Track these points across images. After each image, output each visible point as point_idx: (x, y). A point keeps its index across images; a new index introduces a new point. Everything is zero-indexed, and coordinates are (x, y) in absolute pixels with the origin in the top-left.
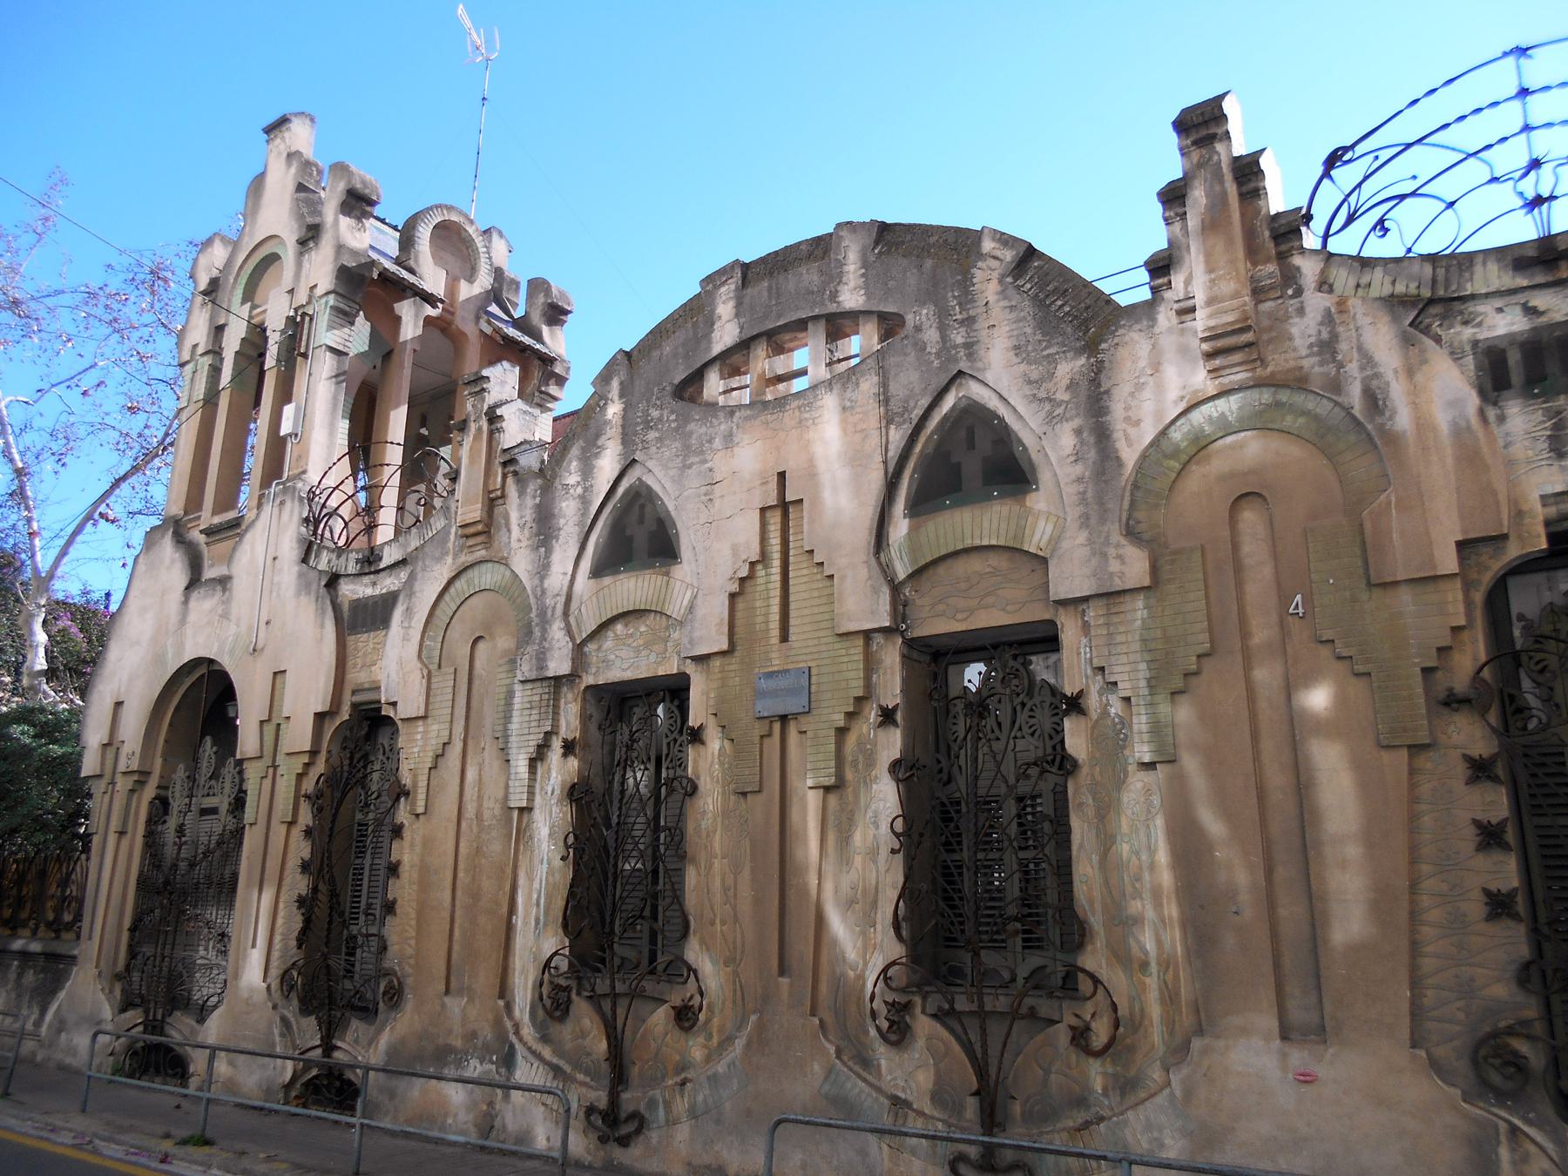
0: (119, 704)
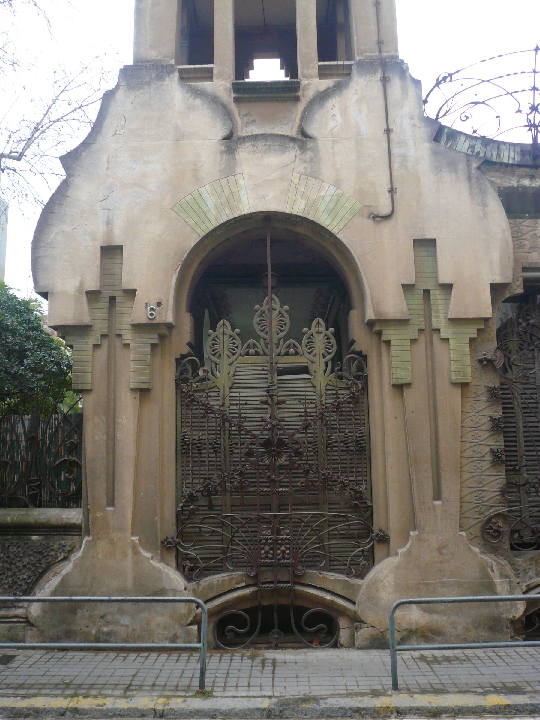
0: (111, 252)
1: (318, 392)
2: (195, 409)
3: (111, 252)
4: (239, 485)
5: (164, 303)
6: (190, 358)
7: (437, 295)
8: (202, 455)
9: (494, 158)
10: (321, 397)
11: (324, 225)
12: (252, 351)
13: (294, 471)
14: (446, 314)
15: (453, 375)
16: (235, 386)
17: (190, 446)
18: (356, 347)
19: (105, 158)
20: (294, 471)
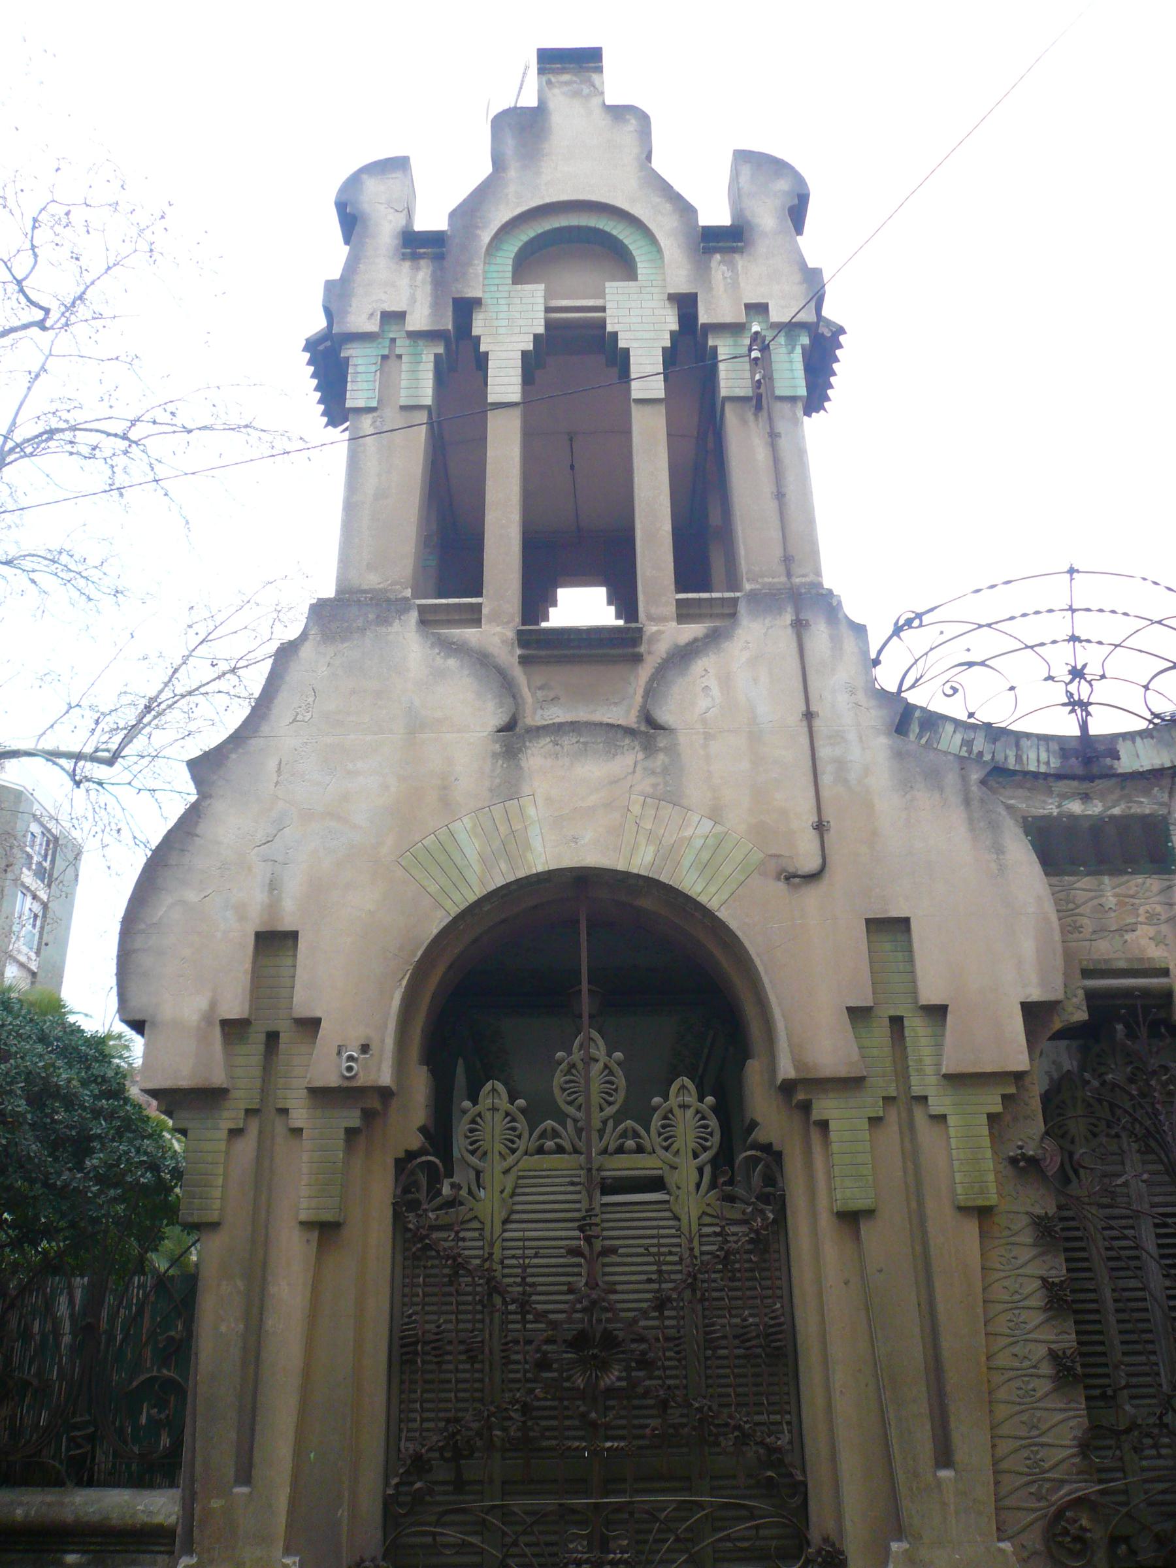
0: (274, 943)
1: (685, 1229)
2: (432, 1267)
3: (274, 943)
4: (519, 1434)
5: (374, 1047)
6: (424, 1158)
7: (917, 1029)
8: (445, 1367)
9: (1011, 764)
10: (691, 1241)
11: (692, 893)
12: (549, 1144)
13: (636, 1402)
14: (938, 1065)
15: (959, 1190)
16: (515, 1217)
17: (419, 1348)
18: (760, 1136)
19: (272, 765)
20: (636, 1402)
